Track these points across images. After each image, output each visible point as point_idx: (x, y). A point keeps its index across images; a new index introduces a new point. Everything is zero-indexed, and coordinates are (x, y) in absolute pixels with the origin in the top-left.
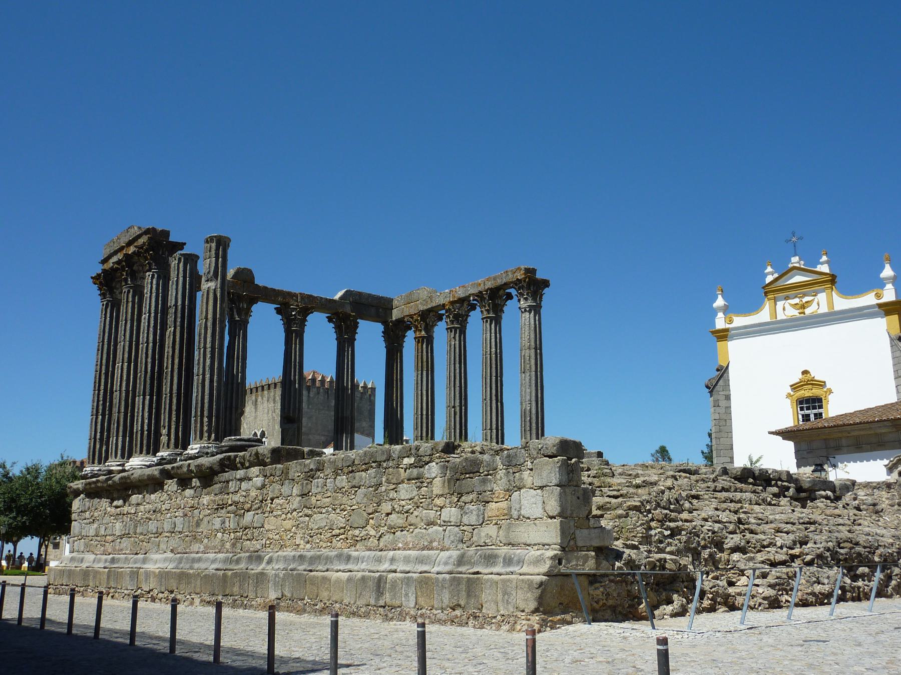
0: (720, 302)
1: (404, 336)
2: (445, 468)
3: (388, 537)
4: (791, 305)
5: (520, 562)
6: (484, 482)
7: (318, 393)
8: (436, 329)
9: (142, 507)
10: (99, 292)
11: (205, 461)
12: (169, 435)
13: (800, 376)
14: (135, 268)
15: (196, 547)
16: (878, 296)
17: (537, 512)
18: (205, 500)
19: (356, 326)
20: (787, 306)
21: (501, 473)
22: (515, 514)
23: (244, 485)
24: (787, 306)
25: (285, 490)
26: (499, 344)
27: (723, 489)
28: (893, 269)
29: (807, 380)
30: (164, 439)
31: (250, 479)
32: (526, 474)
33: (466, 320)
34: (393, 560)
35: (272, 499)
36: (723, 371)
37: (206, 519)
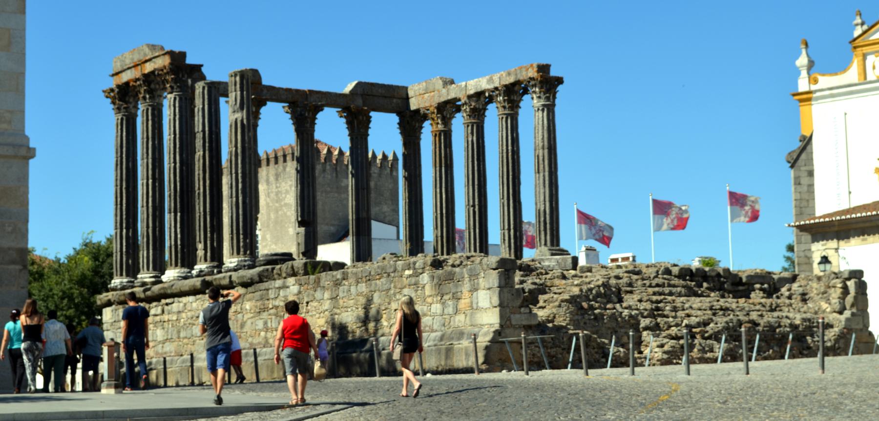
1: (421, 128)
2: (433, 277)
8: (454, 121)
9: (184, 315)
10: (112, 106)
12: (205, 249)
14: (152, 86)
19: (368, 120)
21: (467, 280)
22: (475, 306)
25: (318, 295)
26: (515, 141)
27: (658, 285)
30: (200, 253)
31: (288, 287)
32: (481, 280)
33: (484, 114)
35: (307, 303)
36: (807, 142)
37: (249, 322)
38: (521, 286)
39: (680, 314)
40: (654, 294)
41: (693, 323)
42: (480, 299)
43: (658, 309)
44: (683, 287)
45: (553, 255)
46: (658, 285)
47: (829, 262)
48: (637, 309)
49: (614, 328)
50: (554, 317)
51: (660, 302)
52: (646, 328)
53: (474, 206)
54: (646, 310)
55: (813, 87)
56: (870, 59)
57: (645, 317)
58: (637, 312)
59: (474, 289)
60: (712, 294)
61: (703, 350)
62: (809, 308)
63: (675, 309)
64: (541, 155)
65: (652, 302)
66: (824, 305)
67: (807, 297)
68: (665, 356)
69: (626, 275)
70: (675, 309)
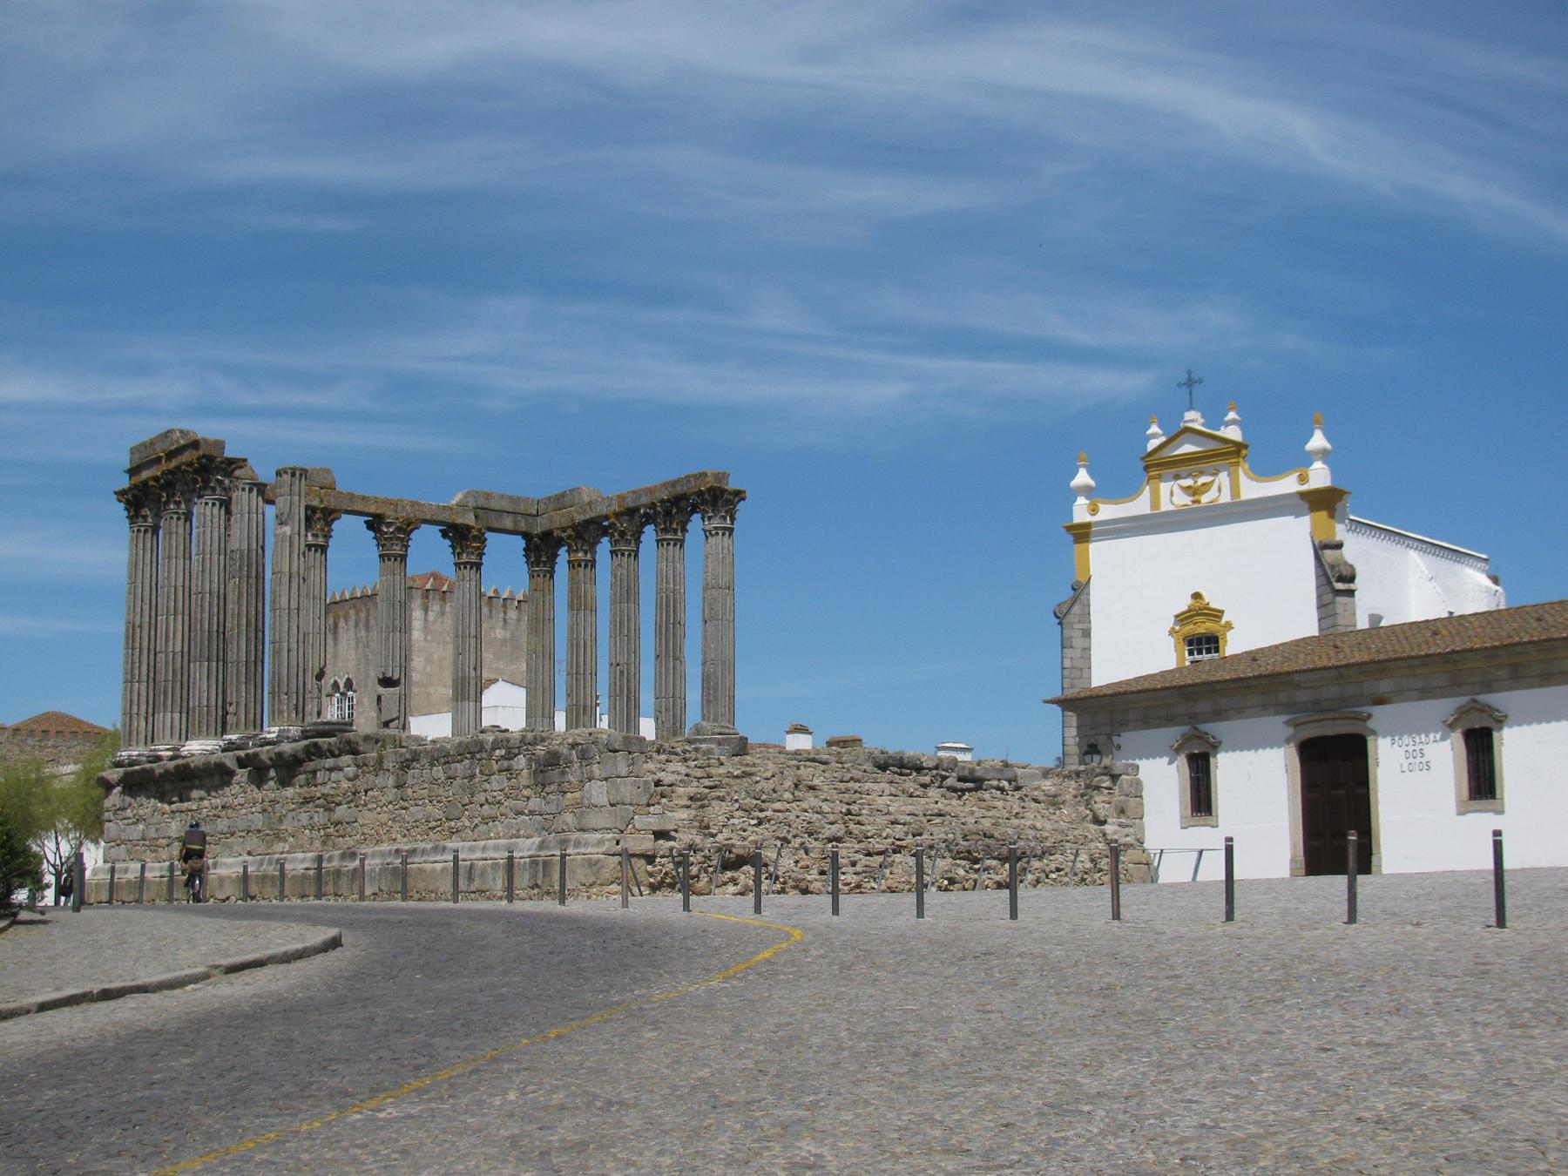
0: (1082, 478)
2: (530, 760)
3: (483, 828)
5: (586, 844)
6: (563, 773)
7: (443, 613)
8: (599, 548)
11: (286, 748)
15: (279, 846)
16: (1303, 479)
17: (604, 800)
18: (290, 791)
20: (1177, 490)
23: (334, 775)
25: (379, 781)
28: (1327, 436)
29: (1199, 610)
34: (484, 849)
36: (1080, 590)
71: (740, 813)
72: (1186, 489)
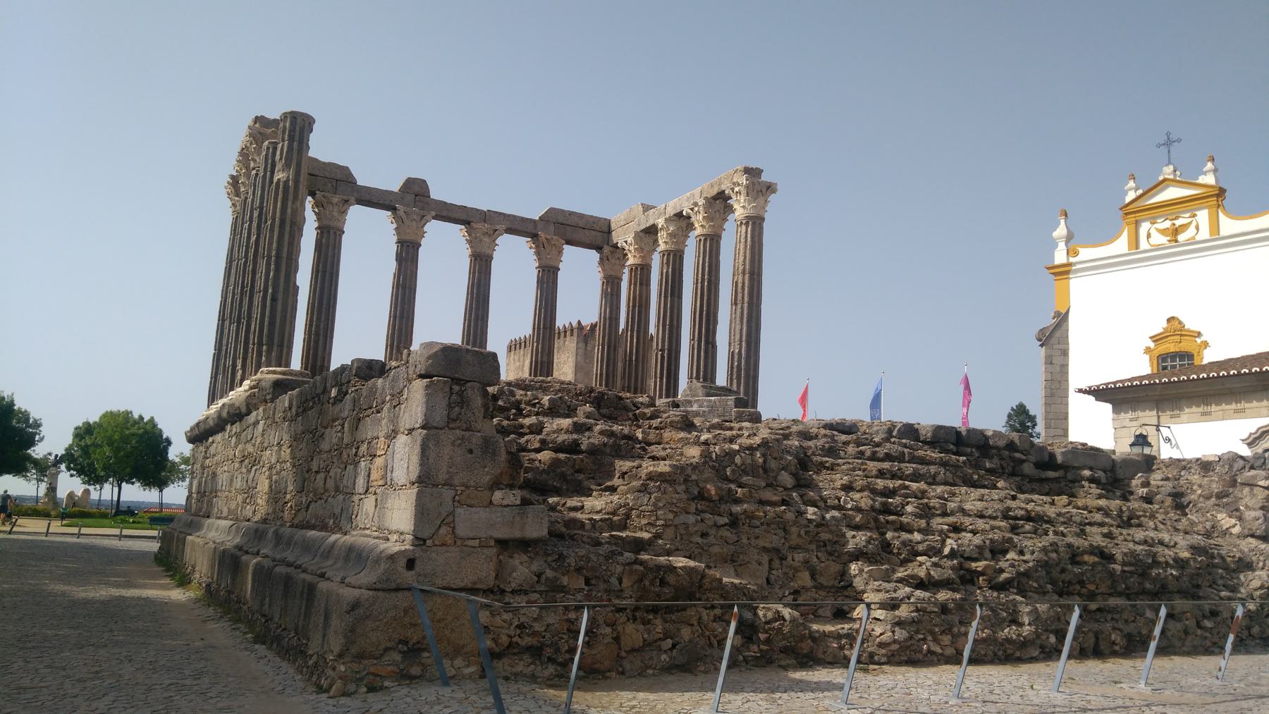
4: (1158, 230)
13: (1165, 325)
24: (1153, 232)
27: (888, 457)
29: (1175, 327)
36: (1062, 319)
38: (575, 436)
39: (938, 523)
40: (881, 474)
41: (968, 550)
42: (397, 456)
43: (886, 510)
44: (944, 464)
45: (708, 395)
46: (888, 457)
47: (1149, 445)
48: (839, 508)
49: (777, 550)
50: (628, 516)
51: (892, 493)
52: (858, 555)
53: (662, 350)
54: (858, 509)
55: (1072, 260)
56: (1145, 227)
57: (857, 528)
58: (836, 513)
59: (393, 435)
60: (1001, 484)
61: (992, 622)
62: (1192, 524)
63: (926, 512)
64: (740, 281)
65: (874, 491)
66: (1225, 520)
67: (1185, 500)
68: (900, 634)
69: (823, 431)
70: (926, 512)
71: (701, 505)
72: (1163, 232)
